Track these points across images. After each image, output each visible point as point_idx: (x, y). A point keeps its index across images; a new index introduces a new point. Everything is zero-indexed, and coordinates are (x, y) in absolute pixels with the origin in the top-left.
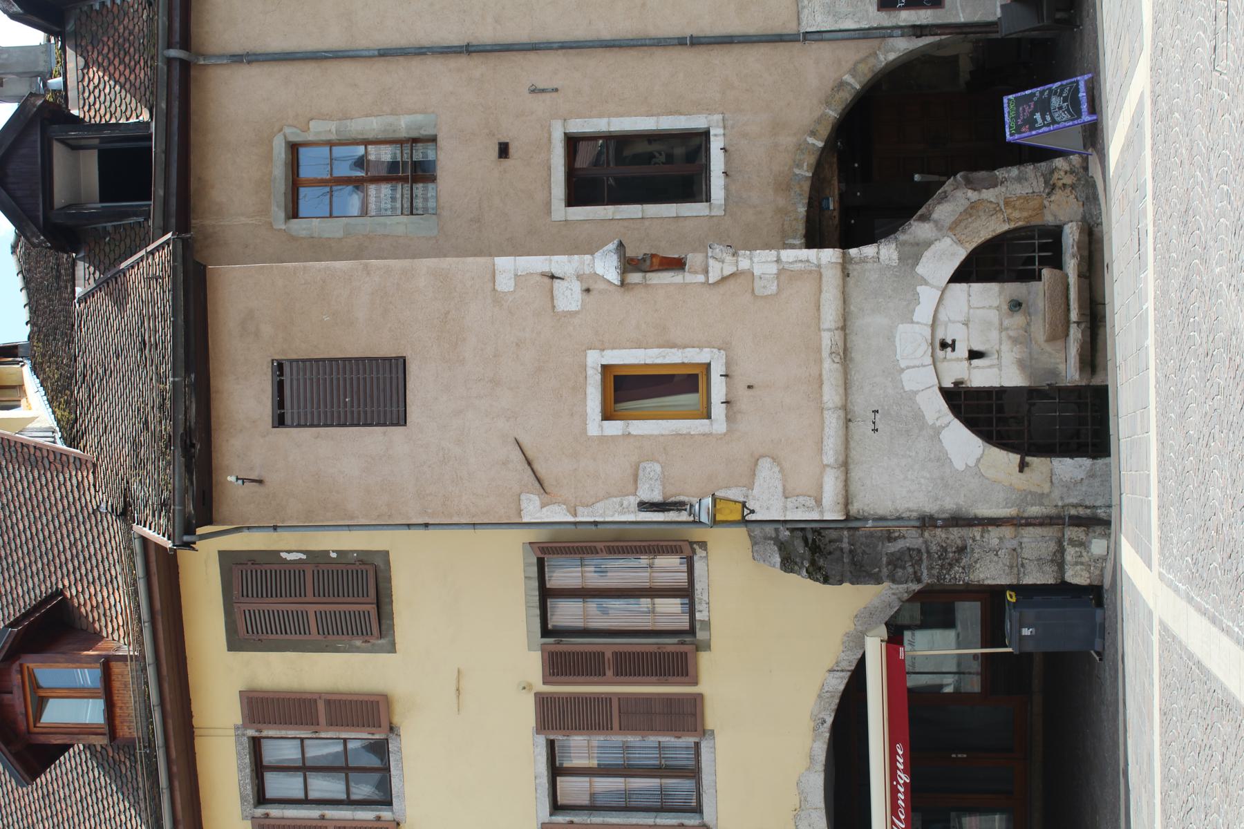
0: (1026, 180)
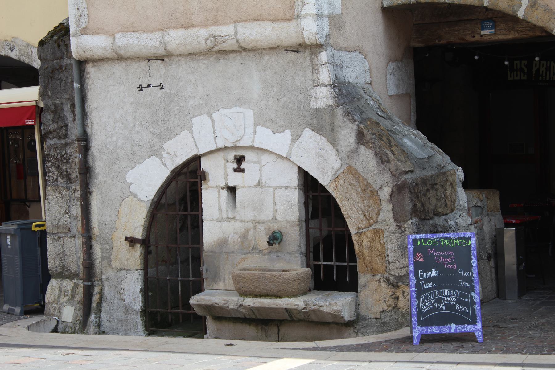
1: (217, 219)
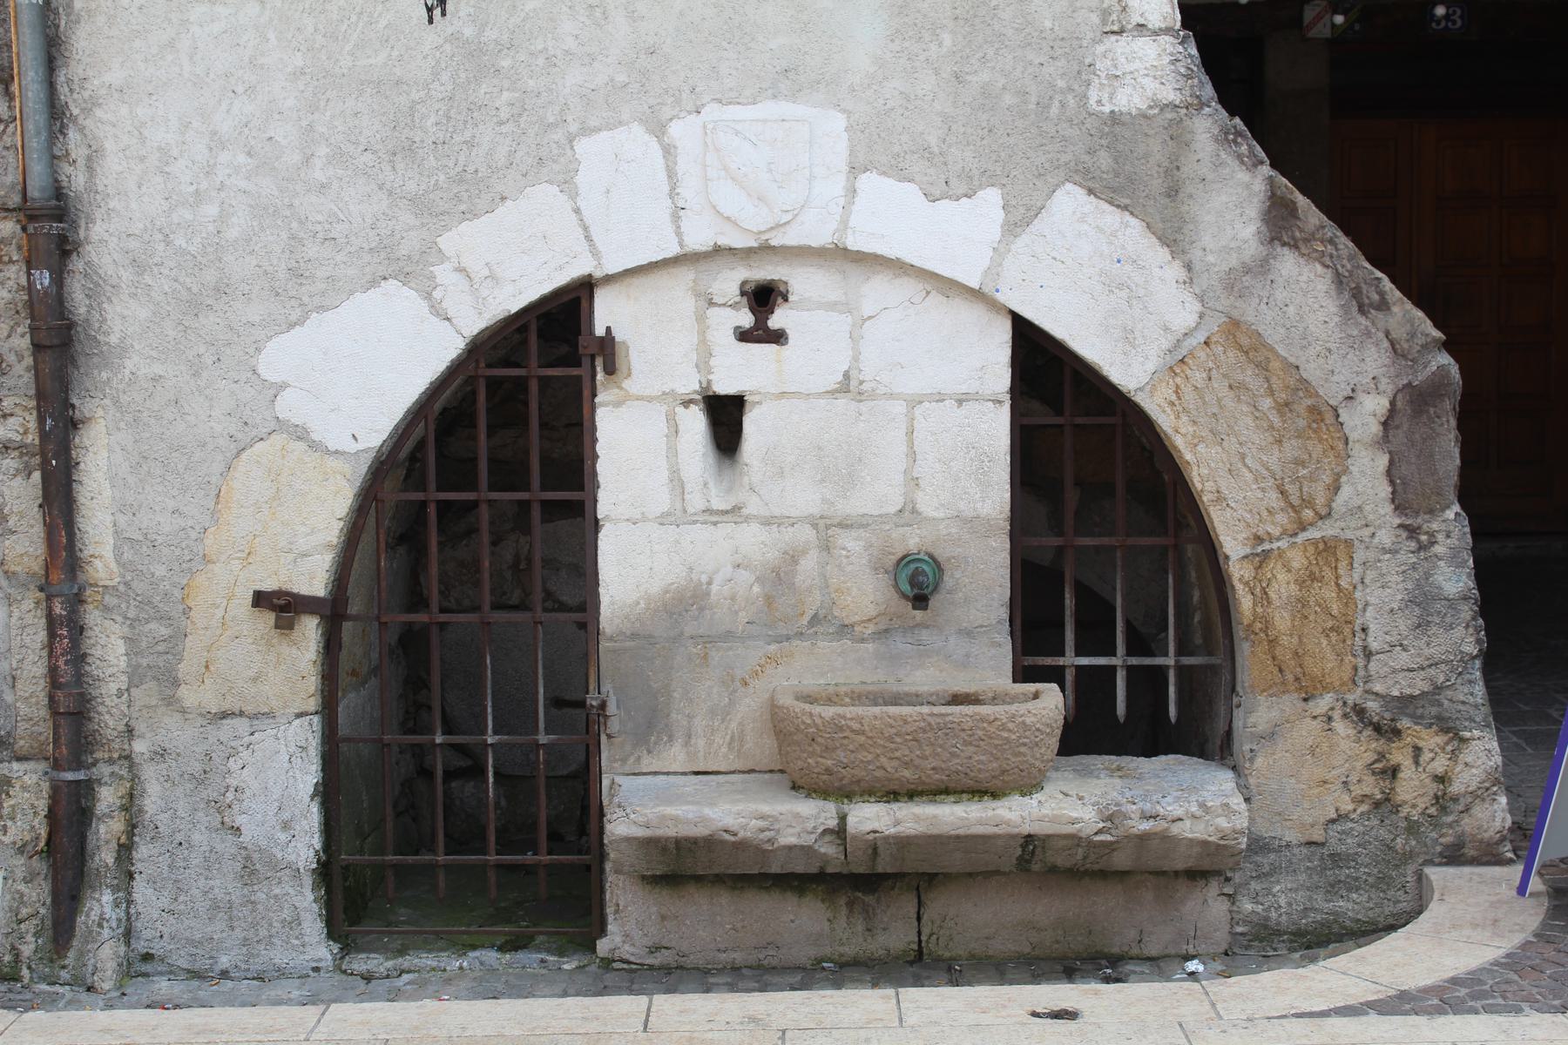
0: (1421, 626)
1: (662, 516)
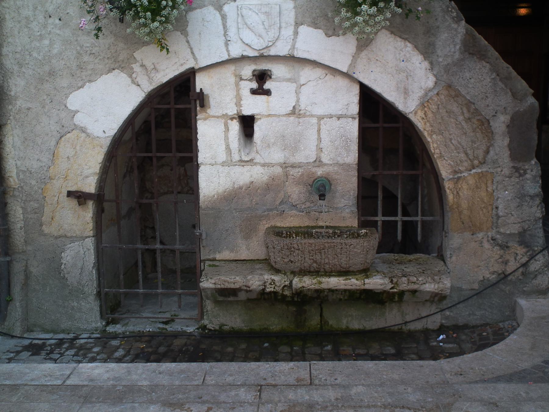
0: (519, 206)
